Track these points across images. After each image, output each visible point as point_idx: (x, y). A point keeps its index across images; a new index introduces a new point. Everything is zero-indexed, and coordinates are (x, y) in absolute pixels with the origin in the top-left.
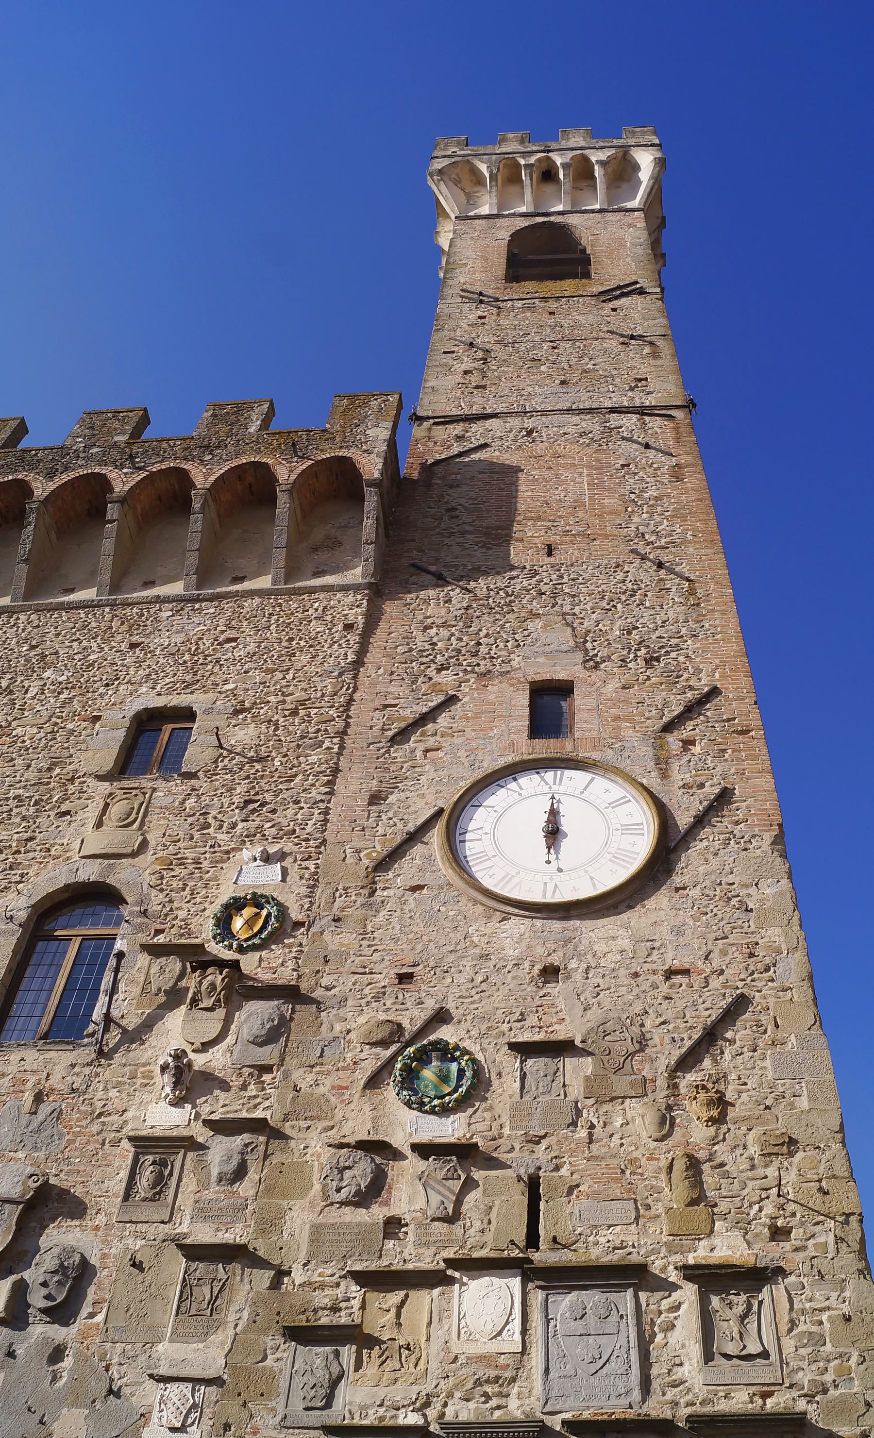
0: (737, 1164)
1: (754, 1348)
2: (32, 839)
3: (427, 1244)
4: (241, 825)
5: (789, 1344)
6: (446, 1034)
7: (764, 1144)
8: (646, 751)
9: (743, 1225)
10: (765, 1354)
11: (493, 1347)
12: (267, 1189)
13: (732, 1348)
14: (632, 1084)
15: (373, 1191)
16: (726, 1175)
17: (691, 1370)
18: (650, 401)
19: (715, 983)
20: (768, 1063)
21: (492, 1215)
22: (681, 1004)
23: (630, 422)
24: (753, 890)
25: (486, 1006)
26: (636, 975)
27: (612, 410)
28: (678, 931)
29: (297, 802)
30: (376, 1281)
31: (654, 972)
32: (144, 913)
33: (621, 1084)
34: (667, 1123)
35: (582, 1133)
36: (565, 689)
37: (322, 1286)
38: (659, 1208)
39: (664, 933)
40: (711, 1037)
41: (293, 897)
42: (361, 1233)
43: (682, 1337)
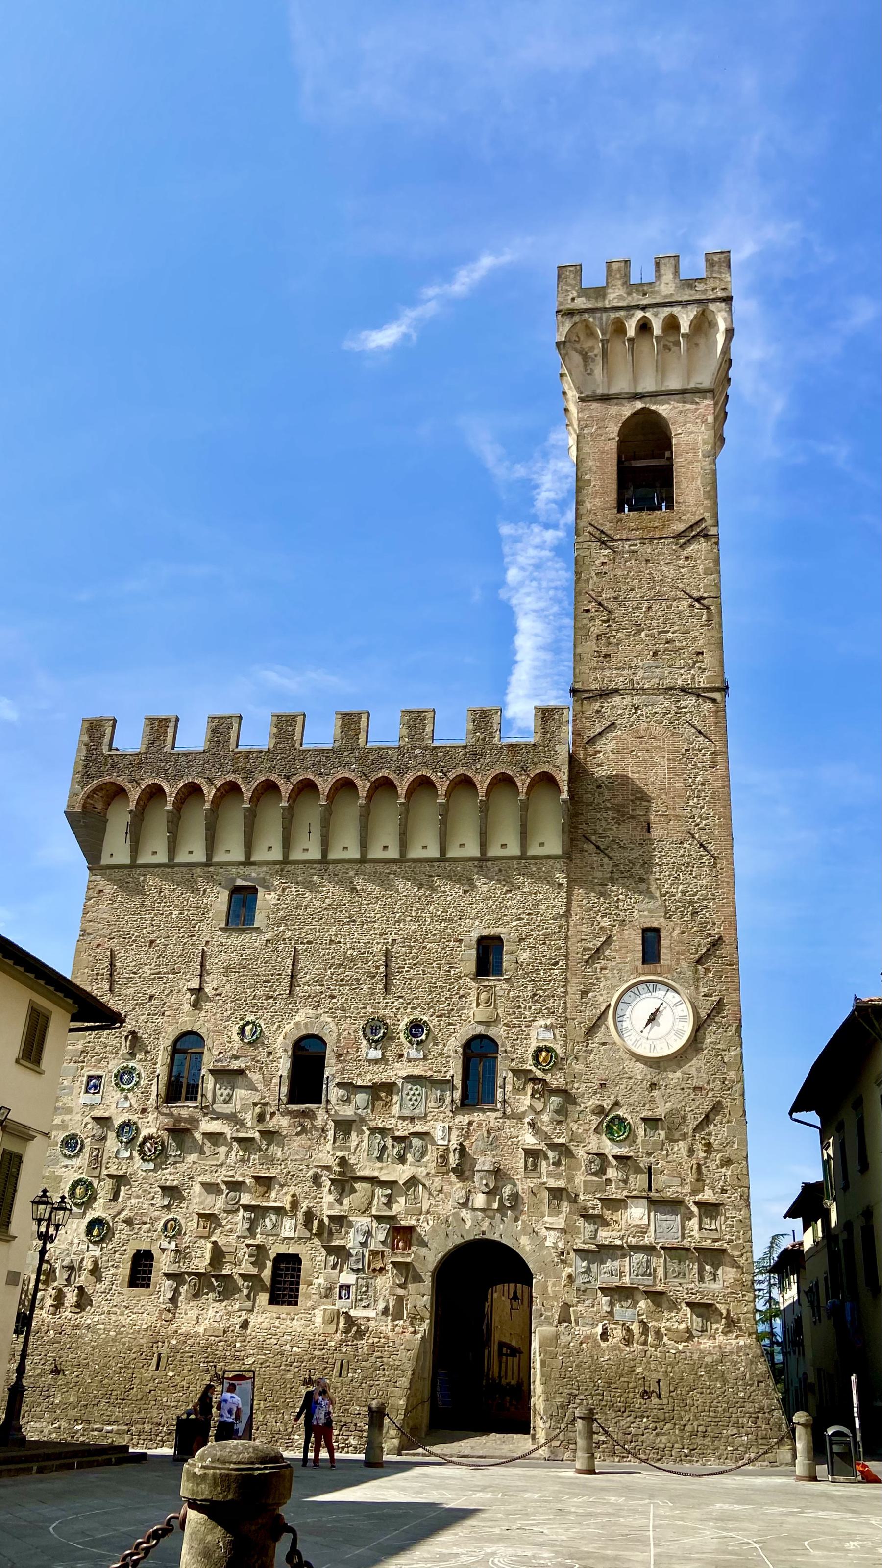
0: (713, 1166)
1: (713, 1227)
2: (453, 1010)
3: (619, 1188)
4: (533, 1007)
5: (723, 1227)
6: (621, 1112)
7: (722, 1161)
8: (689, 974)
9: (713, 1188)
10: (716, 1230)
11: (639, 1222)
12: (569, 1167)
13: (707, 1227)
14: (681, 1135)
15: (602, 1171)
16: (709, 1171)
17: (696, 1233)
18: (703, 682)
19: (710, 1094)
20: (725, 1129)
21: (638, 1182)
22: (698, 1103)
23: (691, 701)
24: (726, 1053)
25: (631, 1101)
26: (683, 1089)
27: (683, 690)
28: (698, 1070)
29: (553, 996)
30: (607, 1202)
31: (689, 1088)
32: (506, 1051)
33: (677, 1135)
34: (691, 1151)
35: (665, 1152)
36: (657, 931)
37: (590, 1200)
38: (688, 1181)
39: (693, 1071)
40: (707, 1120)
41: (559, 1046)
42: (599, 1184)
43: (694, 1223)
